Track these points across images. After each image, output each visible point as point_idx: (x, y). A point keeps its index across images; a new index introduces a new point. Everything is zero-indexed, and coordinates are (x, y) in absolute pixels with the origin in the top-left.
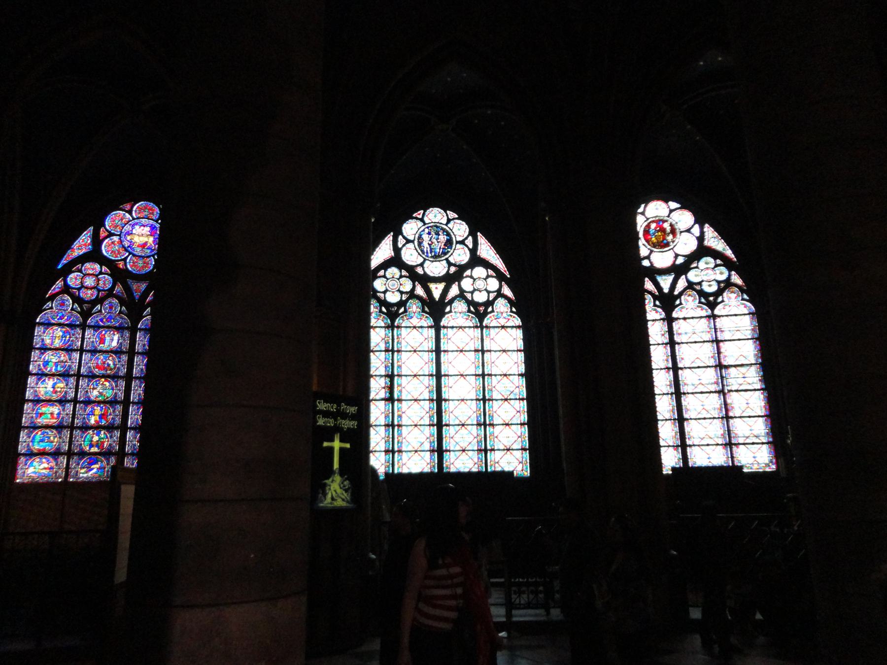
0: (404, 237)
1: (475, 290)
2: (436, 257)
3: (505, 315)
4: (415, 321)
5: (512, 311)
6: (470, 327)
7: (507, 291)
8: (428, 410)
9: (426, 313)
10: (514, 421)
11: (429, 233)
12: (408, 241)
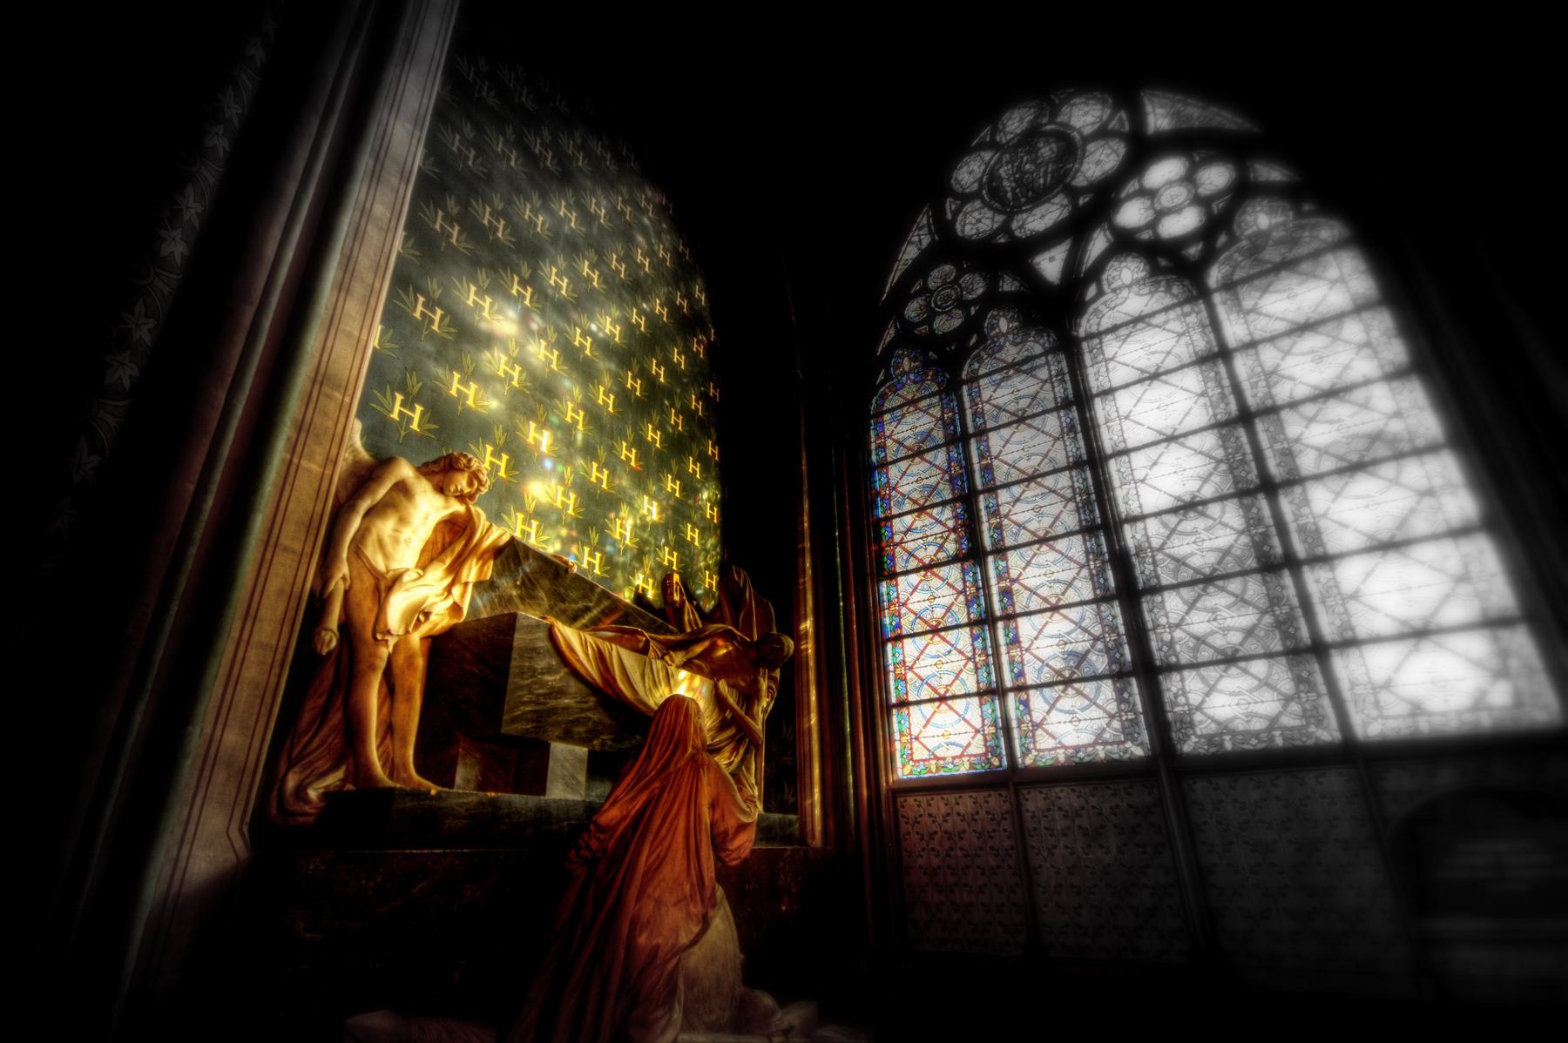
1: (1160, 214)
2: (1037, 196)
4: (1010, 353)
7: (1270, 173)
10: (1420, 526)
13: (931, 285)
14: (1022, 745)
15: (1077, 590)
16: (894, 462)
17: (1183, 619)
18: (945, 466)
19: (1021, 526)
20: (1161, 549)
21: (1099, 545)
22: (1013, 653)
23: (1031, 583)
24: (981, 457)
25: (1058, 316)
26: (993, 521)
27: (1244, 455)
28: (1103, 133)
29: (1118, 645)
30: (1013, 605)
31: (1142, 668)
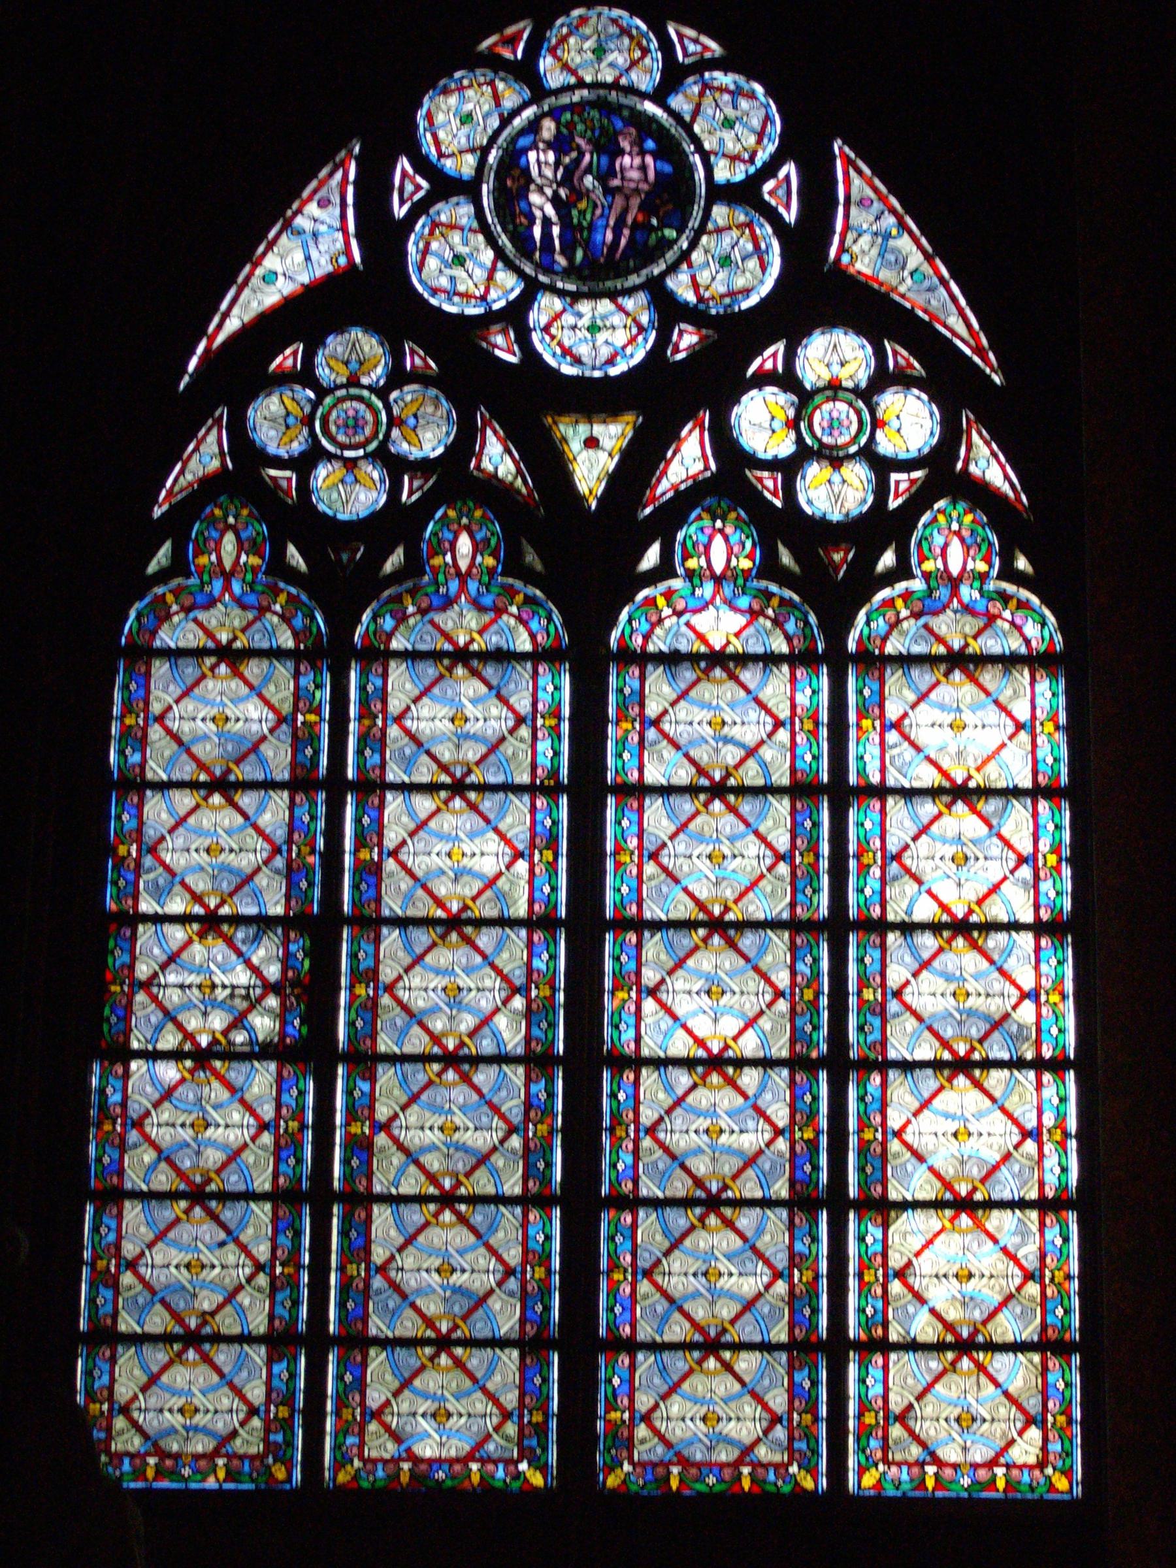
0: (423, 165)
1: (804, 454)
2: (597, 276)
3: (967, 593)
4: (464, 625)
5: (1008, 573)
6: (770, 660)
7: (988, 465)
8: (516, 1117)
9: (529, 576)
10: (1006, 1187)
11: (560, 145)
12: (445, 186)
14: (336, 1447)
15: (495, 1173)
16: (163, 787)
18: (280, 835)
20: (651, 1131)
21: (551, 1095)
22: (352, 1269)
23: (413, 1138)
24: (360, 842)
25: (583, 565)
26: (360, 990)
30: (370, 1176)
31: (574, 1338)
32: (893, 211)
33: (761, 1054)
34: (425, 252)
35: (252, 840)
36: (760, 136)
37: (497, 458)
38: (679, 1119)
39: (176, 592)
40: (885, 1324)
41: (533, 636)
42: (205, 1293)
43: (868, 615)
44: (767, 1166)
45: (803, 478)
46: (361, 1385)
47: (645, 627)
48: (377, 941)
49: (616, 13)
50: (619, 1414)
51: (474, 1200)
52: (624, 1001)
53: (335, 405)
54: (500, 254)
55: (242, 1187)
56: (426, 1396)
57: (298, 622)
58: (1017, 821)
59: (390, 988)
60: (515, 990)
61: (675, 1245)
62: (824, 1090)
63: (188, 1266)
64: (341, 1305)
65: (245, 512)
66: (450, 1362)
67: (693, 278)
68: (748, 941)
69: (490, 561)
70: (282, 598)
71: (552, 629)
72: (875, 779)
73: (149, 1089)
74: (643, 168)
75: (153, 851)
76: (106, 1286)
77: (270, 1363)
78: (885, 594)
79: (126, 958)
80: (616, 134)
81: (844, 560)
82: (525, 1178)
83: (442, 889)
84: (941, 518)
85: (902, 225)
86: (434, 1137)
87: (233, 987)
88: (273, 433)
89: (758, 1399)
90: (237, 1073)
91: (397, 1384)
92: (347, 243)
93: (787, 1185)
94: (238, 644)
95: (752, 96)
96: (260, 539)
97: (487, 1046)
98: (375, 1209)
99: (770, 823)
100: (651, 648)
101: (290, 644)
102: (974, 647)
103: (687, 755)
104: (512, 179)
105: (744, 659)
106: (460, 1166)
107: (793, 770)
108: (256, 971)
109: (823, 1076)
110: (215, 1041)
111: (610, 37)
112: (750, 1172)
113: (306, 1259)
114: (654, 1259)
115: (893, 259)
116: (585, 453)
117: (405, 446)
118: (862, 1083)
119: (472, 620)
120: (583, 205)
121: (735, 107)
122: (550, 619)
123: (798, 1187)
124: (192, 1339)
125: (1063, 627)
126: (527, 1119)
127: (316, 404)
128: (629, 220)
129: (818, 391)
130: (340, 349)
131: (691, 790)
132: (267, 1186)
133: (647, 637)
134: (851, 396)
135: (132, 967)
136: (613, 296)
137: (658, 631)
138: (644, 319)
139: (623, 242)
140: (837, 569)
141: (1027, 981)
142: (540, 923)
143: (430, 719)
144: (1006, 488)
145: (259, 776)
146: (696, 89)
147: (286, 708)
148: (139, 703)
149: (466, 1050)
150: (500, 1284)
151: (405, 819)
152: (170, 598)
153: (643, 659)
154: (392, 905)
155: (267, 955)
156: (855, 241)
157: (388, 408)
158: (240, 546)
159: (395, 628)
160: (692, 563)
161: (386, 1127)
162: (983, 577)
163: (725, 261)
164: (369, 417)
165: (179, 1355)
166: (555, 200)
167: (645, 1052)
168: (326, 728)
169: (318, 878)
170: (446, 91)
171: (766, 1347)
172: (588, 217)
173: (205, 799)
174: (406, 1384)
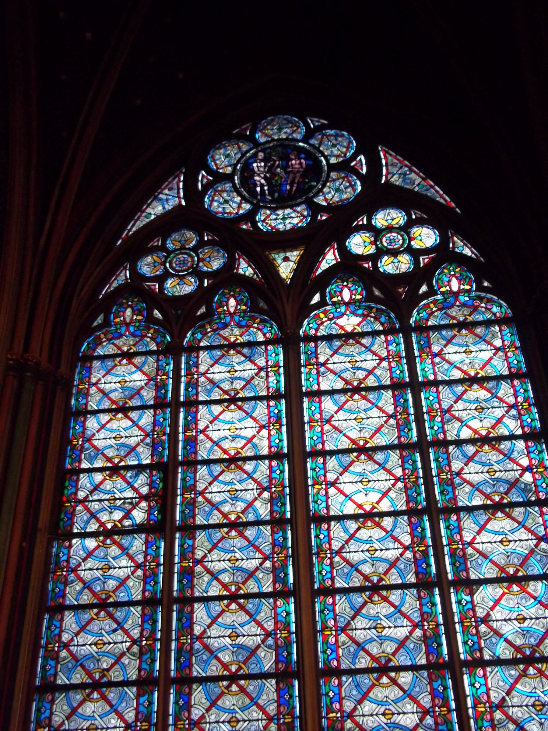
0: (210, 171)
1: (380, 253)
2: (283, 201)
4: (234, 334)
6: (375, 334)
8: (268, 550)
9: (262, 312)
12: (219, 178)
13: (170, 246)
15: (258, 581)
17: (349, 623)
18: (149, 429)
19: (215, 506)
20: (339, 552)
21: (285, 539)
22: (183, 640)
23: (215, 566)
25: (284, 310)
27: (417, 477)
28: (345, 167)
29: (288, 644)
30: (192, 587)
32: (406, 166)
33: (392, 509)
34: (213, 200)
35: (136, 431)
36: (348, 148)
37: (245, 269)
38: (353, 546)
39: (105, 334)
40: (481, 650)
41: (264, 335)
42: (105, 658)
43: (418, 311)
44: (402, 566)
45: (381, 262)
46: (188, 706)
47: (316, 326)
48: (195, 472)
49: (286, 117)
50: (334, 714)
51: (248, 596)
52: (320, 489)
53: (174, 257)
54: (243, 198)
55: (126, 599)
56: (225, 710)
57: (159, 340)
58: (505, 390)
59: (202, 493)
60: (264, 489)
61: (358, 612)
62: (427, 525)
63: (96, 644)
64: (177, 660)
65: (136, 300)
66: (238, 689)
67: (325, 197)
68: (379, 457)
69: (244, 307)
70: (152, 331)
71: (273, 331)
72: (432, 377)
73: (81, 552)
74: (301, 164)
75: (89, 440)
76: (52, 659)
77: (138, 696)
78: (425, 302)
79: (73, 490)
80: (289, 154)
81: (403, 291)
82: (274, 582)
83: (226, 445)
84: (445, 271)
85: (411, 170)
86: (225, 565)
87: (125, 499)
88: (148, 269)
89: (414, 700)
90: (125, 541)
91: (208, 704)
92: (180, 201)
93: (414, 575)
94: (132, 351)
95: (343, 136)
96: (142, 309)
97: (251, 517)
98: (196, 605)
99: (383, 402)
100: (319, 334)
101: (155, 348)
102: (470, 319)
103: (340, 377)
104: (247, 174)
105: (363, 335)
106: (240, 578)
107: (392, 378)
108: (136, 490)
109: (426, 518)
110: (115, 526)
111: (284, 124)
112: (393, 570)
113: (159, 635)
114: (346, 621)
115: (409, 181)
116: (283, 264)
117: (205, 268)
118: (446, 520)
119: (237, 331)
120: (277, 178)
121: (336, 140)
122: (272, 327)
123: (420, 576)
124: (96, 686)
125: (510, 306)
126: (273, 552)
127: (166, 257)
128: (296, 181)
129: (384, 230)
130: (177, 237)
131: (343, 391)
132: (139, 597)
133: (317, 330)
134: (398, 231)
135: (76, 494)
136: (291, 207)
137: (321, 327)
138: (305, 213)
139: (294, 188)
140: (401, 294)
141: (525, 462)
142: (275, 456)
143: (219, 373)
144: (473, 256)
145: (139, 403)
146: (320, 137)
147: (153, 375)
148: (86, 379)
149: (241, 520)
150: (263, 641)
151: (208, 416)
152: (102, 336)
153: (316, 339)
154: (202, 454)
155: (142, 482)
156: (392, 177)
157: (198, 256)
158: (134, 313)
159: (202, 338)
160: (335, 299)
161: (200, 562)
162: (469, 291)
163: (337, 190)
164: (190, 260)
165: (89, 695)
166: (265, 178)
167: (332, 513)
168: (170, 381)
169: (167, 445)
170: (219, 148)
171: (414, 668)
172: (279, 182)
173: (114, 416)
174: (213, 704)
